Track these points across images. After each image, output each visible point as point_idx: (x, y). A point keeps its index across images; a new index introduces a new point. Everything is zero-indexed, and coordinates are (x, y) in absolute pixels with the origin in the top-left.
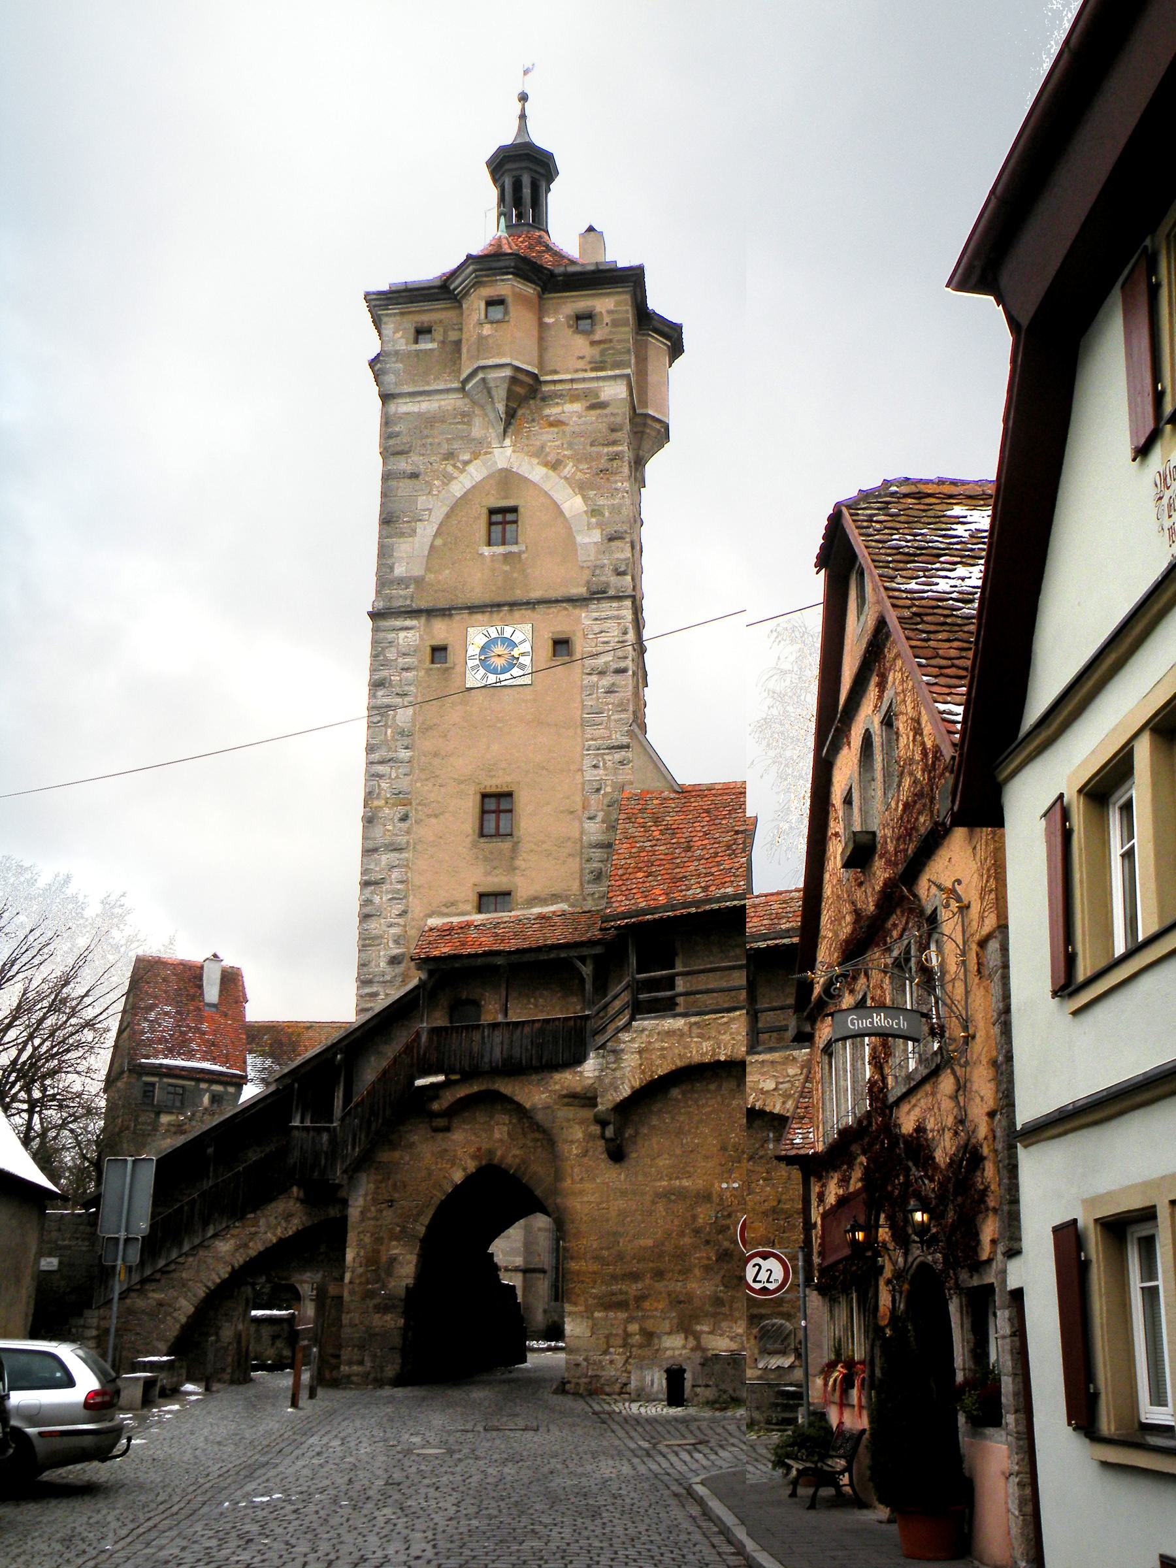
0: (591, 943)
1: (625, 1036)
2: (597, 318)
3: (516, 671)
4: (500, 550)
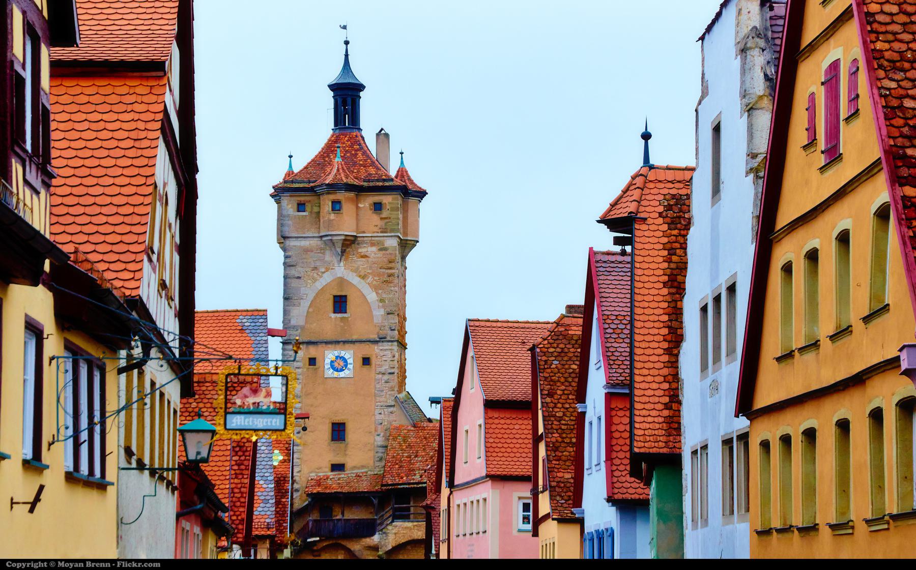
0: (377, 492)
1: (390, 527)
2: (383, 206)
3: (347, 372)
4: (339, 315)
